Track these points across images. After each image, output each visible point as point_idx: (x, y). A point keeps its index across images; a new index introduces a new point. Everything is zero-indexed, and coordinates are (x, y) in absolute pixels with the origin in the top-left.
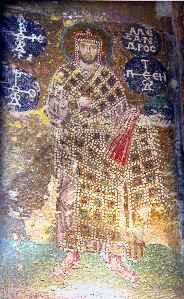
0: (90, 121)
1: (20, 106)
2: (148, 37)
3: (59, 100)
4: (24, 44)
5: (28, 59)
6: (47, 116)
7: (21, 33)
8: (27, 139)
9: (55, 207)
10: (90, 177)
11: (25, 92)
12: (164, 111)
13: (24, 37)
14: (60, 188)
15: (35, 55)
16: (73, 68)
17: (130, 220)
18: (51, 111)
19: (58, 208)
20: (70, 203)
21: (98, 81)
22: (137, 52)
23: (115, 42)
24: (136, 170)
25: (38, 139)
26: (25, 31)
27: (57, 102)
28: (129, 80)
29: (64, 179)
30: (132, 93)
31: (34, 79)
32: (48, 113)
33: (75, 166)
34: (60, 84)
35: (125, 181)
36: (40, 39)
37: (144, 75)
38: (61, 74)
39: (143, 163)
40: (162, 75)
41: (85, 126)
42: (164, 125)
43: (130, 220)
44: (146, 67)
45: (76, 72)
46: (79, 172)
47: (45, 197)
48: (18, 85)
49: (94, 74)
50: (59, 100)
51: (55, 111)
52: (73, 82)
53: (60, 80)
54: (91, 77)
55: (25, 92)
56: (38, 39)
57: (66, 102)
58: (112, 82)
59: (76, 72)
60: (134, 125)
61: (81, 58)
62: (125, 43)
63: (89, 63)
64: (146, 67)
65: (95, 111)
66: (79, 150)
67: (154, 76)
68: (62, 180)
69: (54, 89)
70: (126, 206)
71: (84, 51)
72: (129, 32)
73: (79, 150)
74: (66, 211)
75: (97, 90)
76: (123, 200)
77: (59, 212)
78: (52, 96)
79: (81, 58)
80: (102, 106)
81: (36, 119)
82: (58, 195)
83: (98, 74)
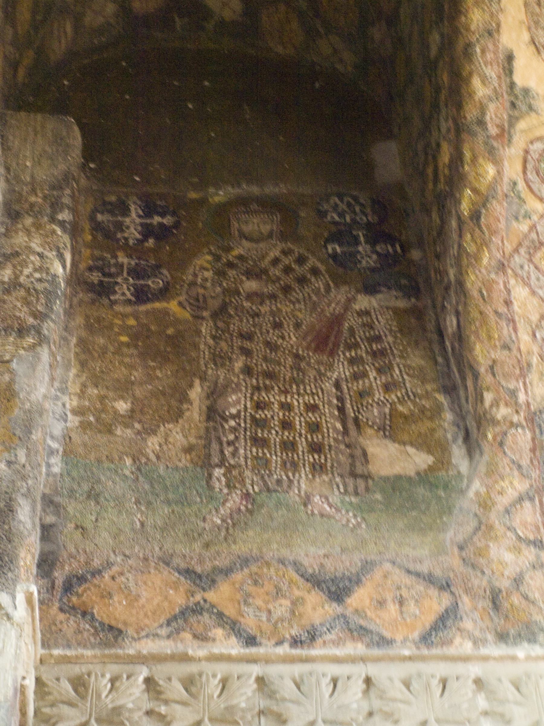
0: (264, 309)
1: (133, 299)
2: (362, 205)
3: (205, 288)
4: (140, 228)
5: (146, 244)
6: (184, 308)
7: (134, 215)
8: (148, 337)
9: (203, 418)
10: (270, 375)
11: (142, 282)
12: (400, 288)
13: (138, 220)
14: (212, 393)
15: (158, 238)
16: (228, 249)
17: (351, 426)
18: (191, 301)
19: (209, 418)
20: (234, 411)
21: (276, 261)
22: (345, 224)
23: (303, 214)
24: (352, 361)
25: (169, 337)
26: (141, 213)
27: (201, 291)
28: (334, 256)
29: (221, 380)
30: (341, 271)
31: (158, 267)
32: (186, 304)
33: (238, 365)
34: (207, 270)
35: (335, 376)
36: (168, 220)
37: (360, 249)
38: (209, 258)
39: (367, 352)
40: (393, 246)
41: (257, 315)
42: (402, 304)
43: (351, 426)
44: (362, 239)
45: (235, 252)
46: (248, 371)
47: (185, 406)
48: (129, 274)
49: (267, 254)
50: (205, 288)
51: (198, 300)
52: (230, 265)
53: (206, 265)
54: (264, 257)
55: (142, 282)
56: (165, 221)
57: (218, 289)
58: (301, 260)
59: (235, 252)
60: (346, 308)
61: (243, 236)
62: (322, 214)
63: (257, 241)
64: (362, 239)
65: (273, 297)
66: (248, 344)
67: (378, 248)
68: (216, 383)
69: (195, 275)
70: (341, 410)
71: (247, 229)
72: (328, 201)
73: (248, 344)
74: (227, 421)
75: (276, 272)
76: (335, 401)
77: (211, 424)
78: (193, 284)
79: (243, 236)
80: (287, 289)
81: (166, 313)
82: (208, 403)
83: (275, 253)
